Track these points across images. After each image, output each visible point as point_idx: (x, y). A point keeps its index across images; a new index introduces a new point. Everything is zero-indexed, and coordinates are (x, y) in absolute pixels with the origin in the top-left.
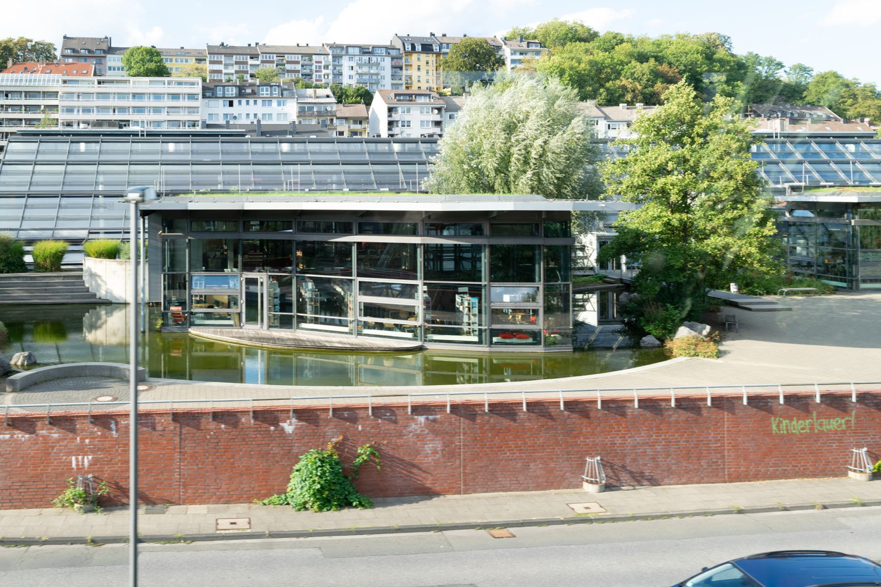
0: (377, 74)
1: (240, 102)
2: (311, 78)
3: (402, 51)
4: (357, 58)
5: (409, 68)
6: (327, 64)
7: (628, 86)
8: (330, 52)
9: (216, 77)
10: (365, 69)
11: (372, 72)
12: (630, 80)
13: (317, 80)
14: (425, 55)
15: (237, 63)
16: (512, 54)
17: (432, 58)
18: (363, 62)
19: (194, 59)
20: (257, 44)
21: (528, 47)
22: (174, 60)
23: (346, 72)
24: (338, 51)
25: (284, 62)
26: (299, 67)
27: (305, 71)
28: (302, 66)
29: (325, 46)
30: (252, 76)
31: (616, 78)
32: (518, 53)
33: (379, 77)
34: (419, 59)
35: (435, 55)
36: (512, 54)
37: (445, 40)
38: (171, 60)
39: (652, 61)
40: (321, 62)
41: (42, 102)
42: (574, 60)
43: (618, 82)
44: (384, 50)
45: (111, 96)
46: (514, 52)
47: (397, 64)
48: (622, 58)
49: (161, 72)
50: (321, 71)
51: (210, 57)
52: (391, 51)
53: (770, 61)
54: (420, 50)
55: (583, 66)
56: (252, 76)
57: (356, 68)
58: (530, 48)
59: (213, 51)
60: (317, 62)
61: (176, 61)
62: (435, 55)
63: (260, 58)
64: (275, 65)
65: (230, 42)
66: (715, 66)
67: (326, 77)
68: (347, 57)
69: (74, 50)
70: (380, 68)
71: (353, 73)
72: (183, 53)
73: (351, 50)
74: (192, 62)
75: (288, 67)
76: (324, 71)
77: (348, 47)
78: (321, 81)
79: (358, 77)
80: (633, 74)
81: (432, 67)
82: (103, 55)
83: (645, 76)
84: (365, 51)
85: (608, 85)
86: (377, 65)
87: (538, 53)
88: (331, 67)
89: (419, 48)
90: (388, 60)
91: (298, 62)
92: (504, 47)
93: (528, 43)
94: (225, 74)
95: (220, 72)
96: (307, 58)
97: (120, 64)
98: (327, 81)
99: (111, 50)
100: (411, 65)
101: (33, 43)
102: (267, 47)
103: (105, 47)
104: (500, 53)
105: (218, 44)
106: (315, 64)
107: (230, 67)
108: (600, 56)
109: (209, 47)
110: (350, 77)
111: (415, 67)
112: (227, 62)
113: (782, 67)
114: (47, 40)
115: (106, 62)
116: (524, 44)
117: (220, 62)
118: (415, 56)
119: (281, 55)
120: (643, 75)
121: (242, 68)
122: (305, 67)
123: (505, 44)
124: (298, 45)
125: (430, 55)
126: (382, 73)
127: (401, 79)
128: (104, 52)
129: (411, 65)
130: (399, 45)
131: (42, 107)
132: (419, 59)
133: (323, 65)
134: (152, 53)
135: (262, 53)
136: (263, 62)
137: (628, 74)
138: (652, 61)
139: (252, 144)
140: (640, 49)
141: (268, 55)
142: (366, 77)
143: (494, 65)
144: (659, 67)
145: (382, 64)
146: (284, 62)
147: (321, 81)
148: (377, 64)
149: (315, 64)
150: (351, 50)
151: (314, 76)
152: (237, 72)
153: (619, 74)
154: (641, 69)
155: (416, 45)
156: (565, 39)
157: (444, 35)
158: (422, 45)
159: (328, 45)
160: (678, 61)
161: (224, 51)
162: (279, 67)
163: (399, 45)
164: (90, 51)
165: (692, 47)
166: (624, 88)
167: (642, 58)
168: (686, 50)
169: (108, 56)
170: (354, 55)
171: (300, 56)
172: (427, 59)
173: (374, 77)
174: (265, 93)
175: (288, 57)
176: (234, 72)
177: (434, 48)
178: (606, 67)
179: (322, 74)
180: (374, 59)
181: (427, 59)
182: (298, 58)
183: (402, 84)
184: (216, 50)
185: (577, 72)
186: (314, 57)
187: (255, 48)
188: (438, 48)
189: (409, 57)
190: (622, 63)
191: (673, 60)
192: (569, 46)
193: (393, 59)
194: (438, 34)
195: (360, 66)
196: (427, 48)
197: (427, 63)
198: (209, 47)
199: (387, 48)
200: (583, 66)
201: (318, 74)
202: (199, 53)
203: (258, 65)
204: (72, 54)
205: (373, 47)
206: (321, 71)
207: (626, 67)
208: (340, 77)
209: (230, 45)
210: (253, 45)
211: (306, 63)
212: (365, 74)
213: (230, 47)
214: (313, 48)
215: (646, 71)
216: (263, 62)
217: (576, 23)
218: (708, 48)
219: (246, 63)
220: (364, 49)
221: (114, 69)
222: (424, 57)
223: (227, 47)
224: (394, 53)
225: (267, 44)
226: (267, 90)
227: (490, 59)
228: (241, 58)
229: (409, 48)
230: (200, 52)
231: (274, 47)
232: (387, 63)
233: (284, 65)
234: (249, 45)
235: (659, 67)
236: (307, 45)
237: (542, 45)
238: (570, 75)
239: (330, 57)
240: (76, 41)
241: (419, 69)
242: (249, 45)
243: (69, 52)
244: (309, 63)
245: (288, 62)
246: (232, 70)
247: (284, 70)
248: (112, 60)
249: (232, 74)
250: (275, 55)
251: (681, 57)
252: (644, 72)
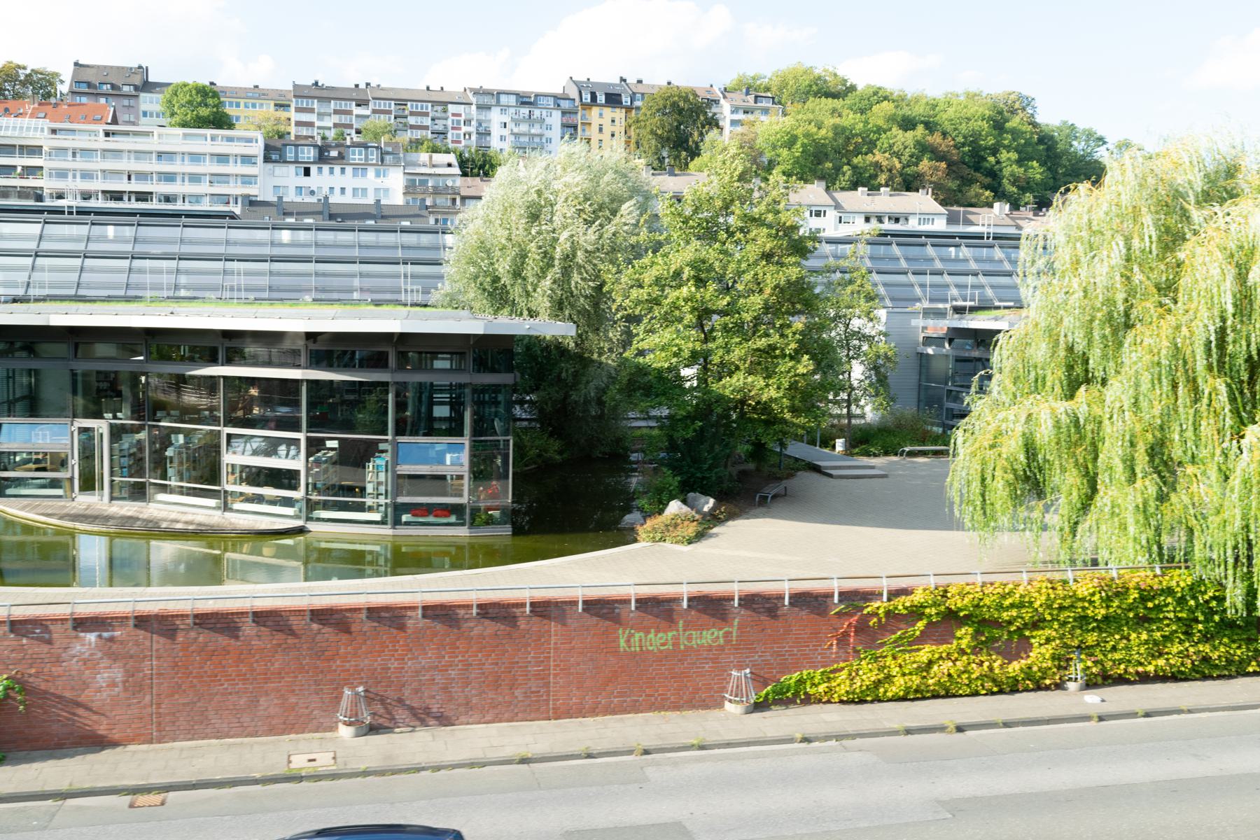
0: (541, 136)
1: (320, 169)
2: (446, 138)
3: (577, 103)
4: (512, 110)
5: (586, 127)
6: (468, 117)
7: (884, 163)
8: (473, 100)
9: (304, 131)
10: (524, 128)
11: (533, 131)
12: (887, 155)
13: (453, 142)
14: (610, 109)
15: (336, 112)
16: (732, 112)
17: (619, 114)
18: (522, 116)
19: (272, 103)
20: (368, 84)
21: (756, 102)
22: (242, 105)
23: (496, 131)
24: (487, 100)
25: (407, 112)
26: (427, 121)
27: (436, 127)
28: (433, 119)
29: (468, 91)
30: (358, 132)
31: (870, 151)
32: (741, 112)
33: (544, 140)
34: (601, 115)
35: (624, 110)
36: (732, 112)
37: (640, 89)
38: (238, 105)
39: (920, 129)
40: (459, 115)
41: (20, 161)
42: (813, 124)
43: (870, 158)
44: (551, 101)
45: (179, 157)
46: (735, 110)
47: (570, 122)
48: (881, 122)
49: (220, 121)
50: (460, 129)
51: (297, 102)
52: (562, 103)
53: (1090, 135)
54: (604, 102)
55: (823, 132)
56: (358, 132)
57: (511, 125)
58: (759, 104)
59: (300, 92)
60: (454, 115)
61: (246, 107)
62: (624, 110)
63: (371, 106)
64: (393, 117)
65: (325, 81)
66: (1005, 139)
67: (467, 137)
68: (498, 109)
69: (89, 85)
70: (544, 127)
71: (506, 132)
72: (257, 94)
73: (503, 99)
74: (269, 109)
75: (412, 120)
76: (464, 129)
77: (499, 93)
78: (459, 142)
79: (512, 138)
80: (891, 146)
81: (619, 128)
82: (134, 93)
83: (907, 150)
84: (525, 100)
85: (855, 161)
86: (542, 121)
87: (766, 111)
88: (474, 123)
89: (601, 99)
90: (557, 115)
91: (426, 114)
92: (722, 101)
93: (756, 97)
94: (319, 128)
95: (311, 124)
96: (439, 108)
97: (157, 108)
98: (468, 143)
99: (148, 86)
100: (590, 124)
101: (28, 72)
102: (382, 89)
103: (137, 80)
104: (714, 110)
105: (310, 82)
106: (451, 118)
107: (326, 118)
108: (850, 119)
109: (295, 86)
110: (502, 138)
111: (595, 128)
112: (322, 111)
113: (1105, 143)
114: (50, 69)
115: (138, 104)
116: (751, 98)
117: (311, 111)
118: (595, 111)
119: (401, 103)
120: (906, 148)
121: (344, 119)
122: (437, 121)
123: (725, 97)
124: (428, 88)
125: (618, 110)
126: (548, 134)
128: (136, 88)
129: (590, 124)
130: (574, 94)
131: (19, 169)
132: (601, 115)
133: (462, 119)
134: (207, 93)
135: (374, 99)
136: (374, 112)
137: (886, 145)
138: (920, 129)
139: (361, 233)
140: (906, 111)
141: (419, 104)
142: (524, 139)
143: (703, 127)
144: (929, 138)
145: (548, 121)
146: (407, 112)
147: (459, 142)
149: (451, 118)
150: (503, 99)
151: (449, 136)
152: (336, 125)
153: (872, 145)
154: (903, 140)
155: (598, 94)
156: (808, 92)
157: (640, 82)
158: (607, 94)
159: (471, 90)
160: (956, 129)
161: (318, 93)
162: (399, 120)
163: (574, 94)
164: (113, 87)
165: (977, 111)
166: (877, 165)
167: (908, 124)
168: (969, 115)
169: (143, 95)
170: (509, 106)
171: (430, 105)
172: (613, 115)
173: (537, 140)
175: (412, 106)
176: (331, 125)
177: (624, 99)
178: (857, 135)
179: (462, 132)
180: (537, 113)
181: (613, 115)
182: (427, 108)
184: (306, 92)
185: (814, 140)
186: (450, 106)
187: (364, 91)
188: (629, 99)
189: (587, 112)
190: (879, 130)
191: (949, 128)
192: (812, 103)
193: (564, 113)
194: (632, 80)
195: (517, 122)
196: (613, 100)
197: (613, 121)
198: (295, 86)
199: (556, 97)
200: (823, 132)
201: (455, 132)
202: (280, 96)
203: (368, 117)
204: (87, 90)
205: (537, 96)
206: (460, 129)
207: (883, 136)
208: (488, 138)
209: (327, 84)
210: (362, 86)
211: (438, 115)
212: (524, 135)
213: (327, 88)
214: (450, 93)
215: (910, 143)
216: (374, 112)
217: (825, 71)
218: (1000, 113)
219: (349, 113)
220: (523, 97)
221: (151, 116)
222: (608, 113)
223: (322, 88)
224: (565, 105)
225: (383, 86)
227: (698, 117)
228: (343, 105)
229: (587, 98)
230: (281, 94)
231: (392, 89)
232: (556, 119)
233: (406, 117)
234: (357, 86)
235: (929, 138)
236: (442, 88)
237: (776, 100)
238: (803, 145)
239: (474, 107)
240: (94, 71)
241: (601, 130)
242: (357, 86)
243: (84, 89)
244: (443, 115)
245: (412, 114)
246: (329, 122)
247: (405, 125)
248: (149, 102)
249: (329, 129)
250: (393, 103)
251: (961, 124)
252: (906, 144)
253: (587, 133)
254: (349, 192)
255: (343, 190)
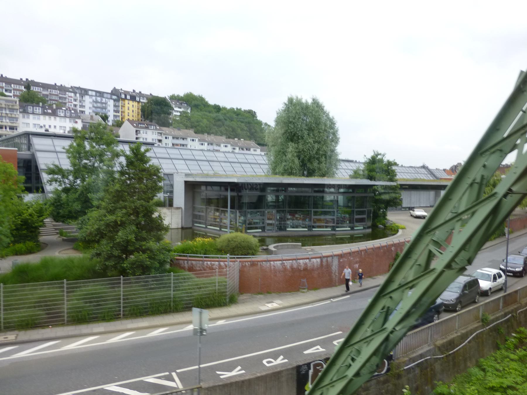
17: (135, 104)
34: (129, 103)
54: (129, 98)
62: (137, 102)
81: (135, 109)
89: (128, 97)
118: (126, 102)
125: (135, 102)
127: (118, 113)
132: (129, 103)
145: (109, 103)
148: (106, 103)
174: (38, 111)
183: (119, 116)
196: (133, 98)
222: (131, 102)
226: (39, 110)
241: (128, 109)
253: (123, 110)
254: (58, 127)
255: (55, 127)
